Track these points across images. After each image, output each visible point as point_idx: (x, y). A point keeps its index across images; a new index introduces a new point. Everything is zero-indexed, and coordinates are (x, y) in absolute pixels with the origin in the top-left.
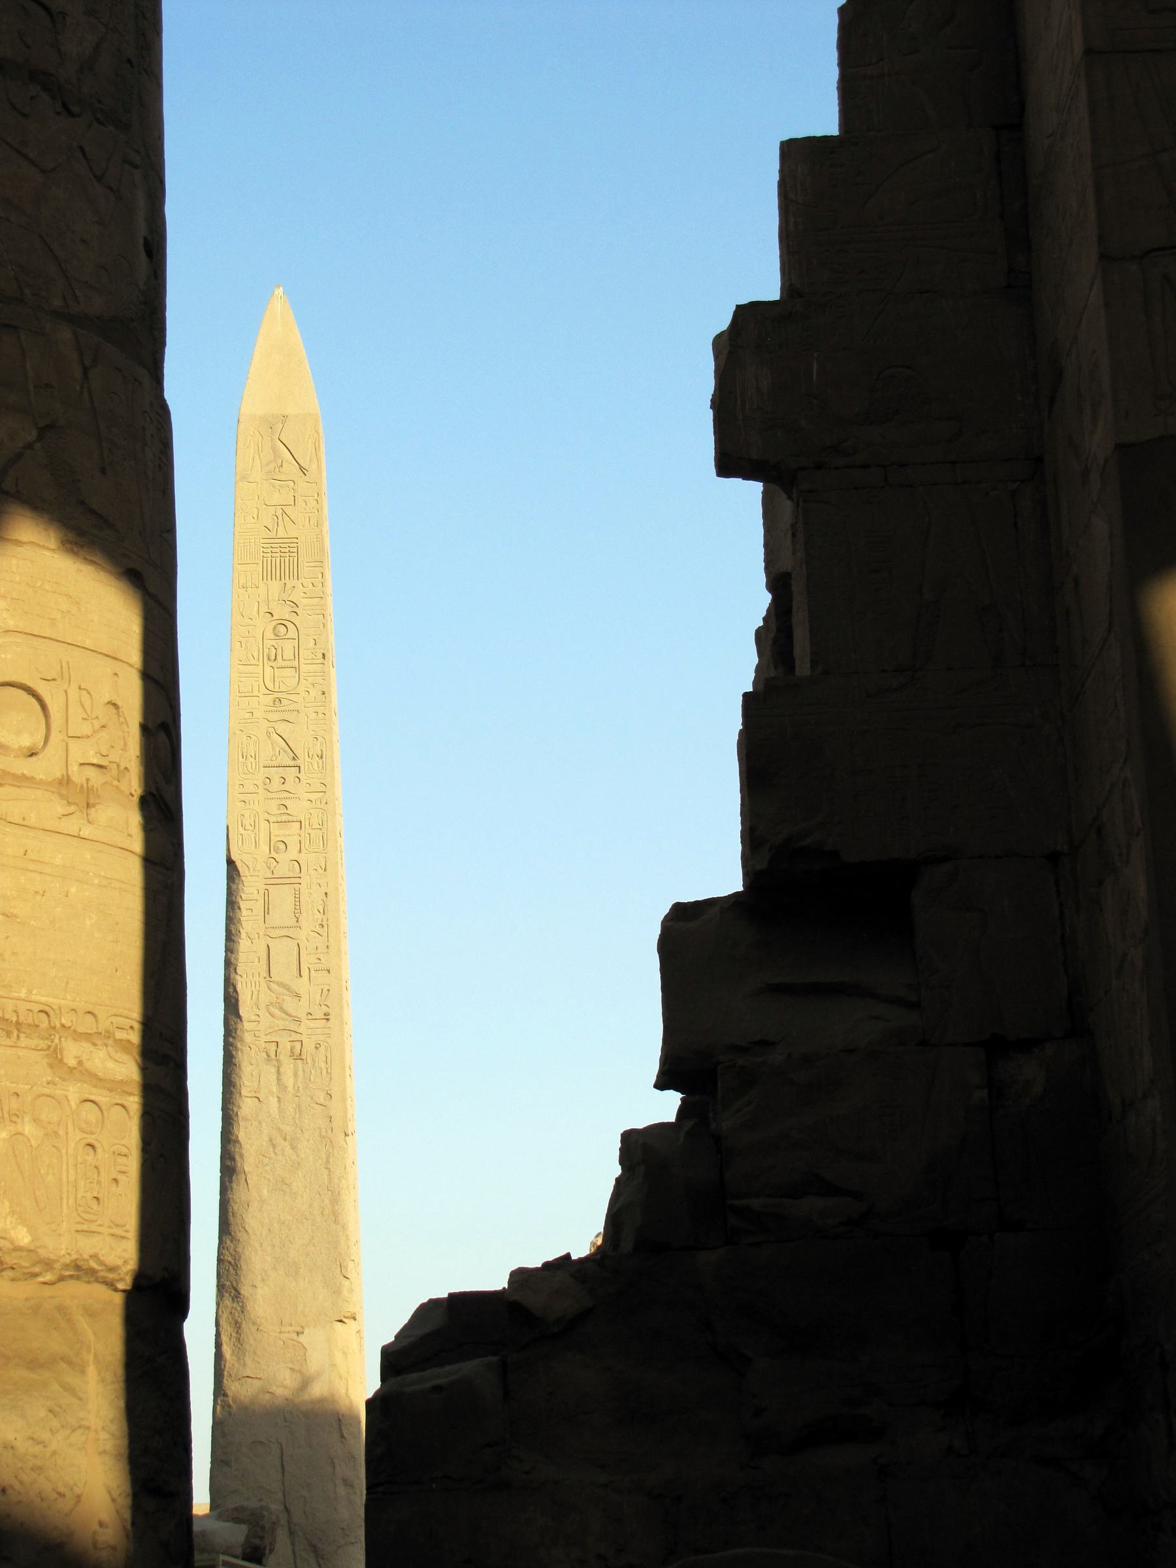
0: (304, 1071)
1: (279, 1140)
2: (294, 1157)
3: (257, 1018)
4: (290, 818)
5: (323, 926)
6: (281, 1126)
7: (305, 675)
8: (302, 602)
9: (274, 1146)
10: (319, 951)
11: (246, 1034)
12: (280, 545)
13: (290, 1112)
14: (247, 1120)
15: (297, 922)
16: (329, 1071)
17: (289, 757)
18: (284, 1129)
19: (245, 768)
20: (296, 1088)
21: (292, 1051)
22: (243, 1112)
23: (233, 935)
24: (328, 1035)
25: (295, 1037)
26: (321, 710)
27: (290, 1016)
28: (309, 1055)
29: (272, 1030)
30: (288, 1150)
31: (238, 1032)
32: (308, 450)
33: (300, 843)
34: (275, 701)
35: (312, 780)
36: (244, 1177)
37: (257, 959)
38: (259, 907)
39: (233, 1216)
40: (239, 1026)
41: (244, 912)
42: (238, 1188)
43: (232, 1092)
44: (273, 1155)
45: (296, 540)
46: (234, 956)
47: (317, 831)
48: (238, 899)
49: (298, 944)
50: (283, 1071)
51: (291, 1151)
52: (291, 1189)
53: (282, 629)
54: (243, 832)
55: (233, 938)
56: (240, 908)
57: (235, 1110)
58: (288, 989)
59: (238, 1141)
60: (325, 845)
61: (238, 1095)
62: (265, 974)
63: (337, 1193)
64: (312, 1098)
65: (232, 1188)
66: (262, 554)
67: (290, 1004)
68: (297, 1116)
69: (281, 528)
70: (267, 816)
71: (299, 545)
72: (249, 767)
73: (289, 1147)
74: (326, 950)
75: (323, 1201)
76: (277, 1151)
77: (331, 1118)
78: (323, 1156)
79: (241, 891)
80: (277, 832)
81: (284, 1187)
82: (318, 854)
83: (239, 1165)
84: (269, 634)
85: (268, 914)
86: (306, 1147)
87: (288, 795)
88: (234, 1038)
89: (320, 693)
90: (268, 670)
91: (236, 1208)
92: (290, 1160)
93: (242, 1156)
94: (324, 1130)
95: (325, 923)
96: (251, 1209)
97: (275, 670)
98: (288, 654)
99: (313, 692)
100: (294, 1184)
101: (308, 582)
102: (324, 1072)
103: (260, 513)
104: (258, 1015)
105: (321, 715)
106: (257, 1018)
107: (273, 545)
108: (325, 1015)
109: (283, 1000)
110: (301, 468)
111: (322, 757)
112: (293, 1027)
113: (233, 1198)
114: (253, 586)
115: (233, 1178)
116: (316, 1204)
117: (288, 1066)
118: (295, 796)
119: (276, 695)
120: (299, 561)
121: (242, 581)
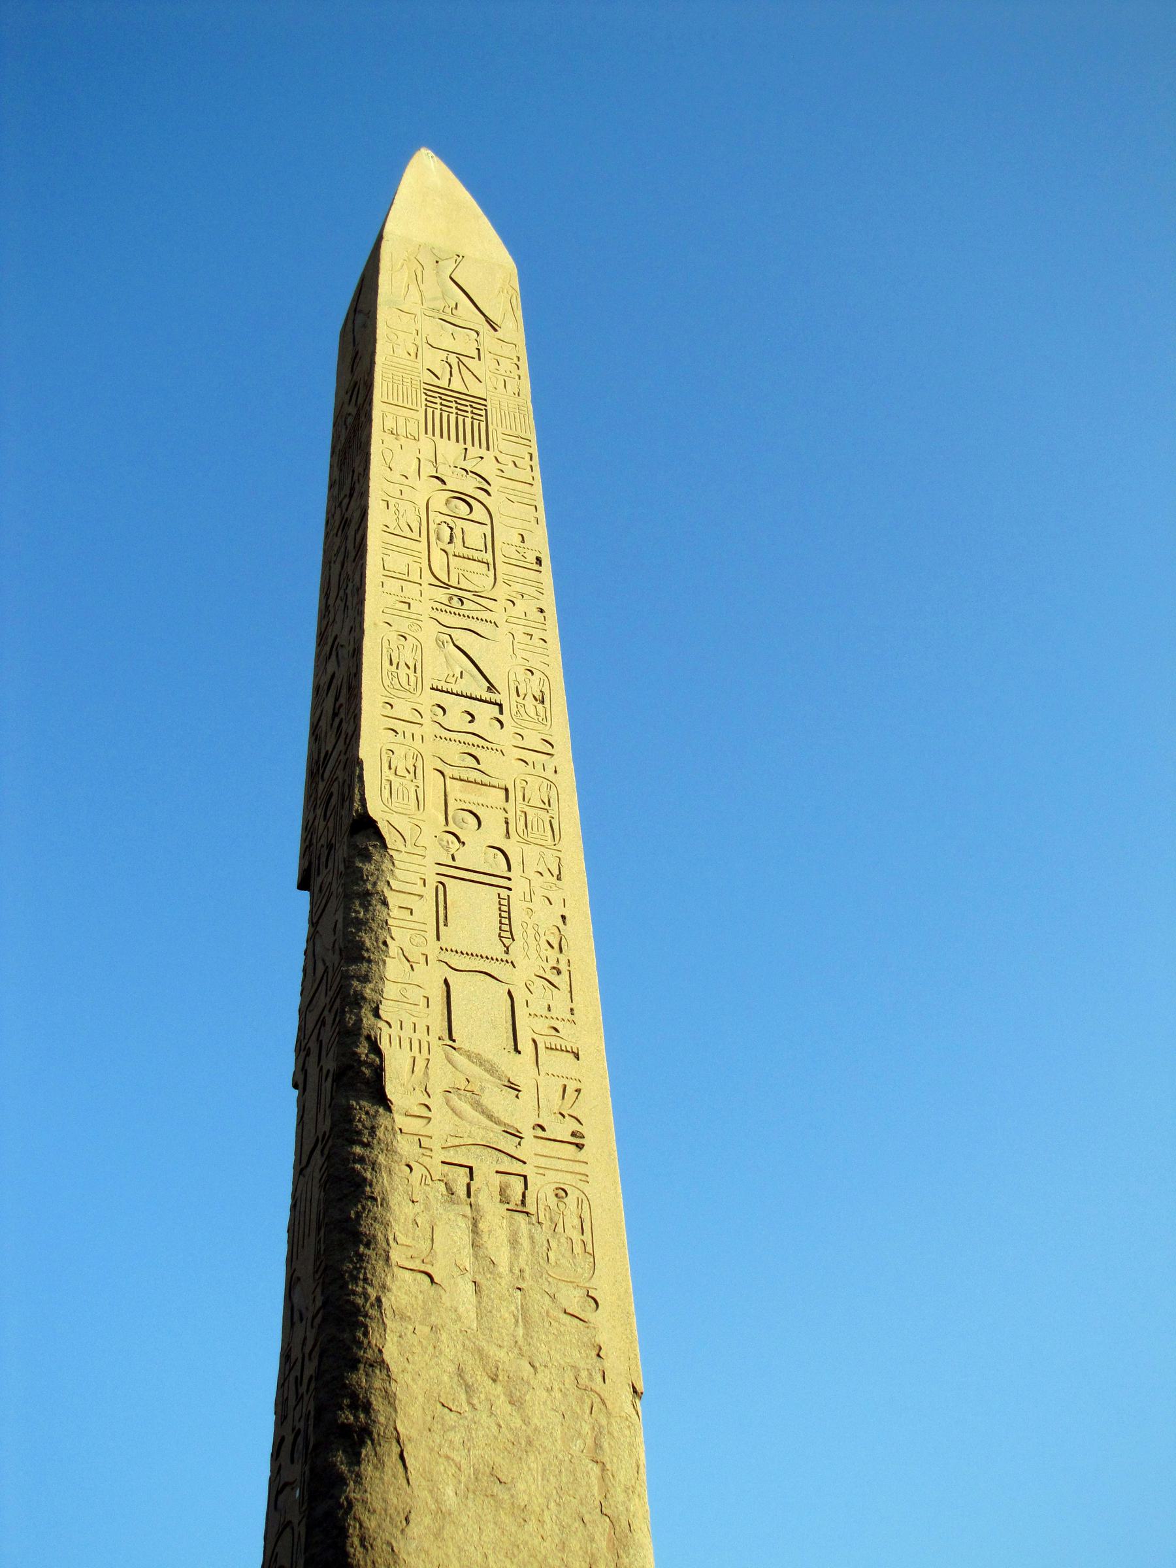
0: (532, 1238)
1: (481, 1379)
2: (517, 1422)
3: (425, 1112)
4: (486, 780)
5: (559, 972)
6: (484, 1344)
9: (469, 1389)
10: (554, 1013)
11: (399, 1136)
13: (505, 1320)
14: (403, 1317)
15: (507, 952)
16: (589, 1249)
18: (491, 1353)
20: (517, 1272)
21: (502, 1191)
22: (393, 1298)
23: (367, 950)
24: (584, 1178)
25: (507, 1165)
26: (537, 634)
27: (498, 1122)
28: (541, 1207)
29: (457, 1141)
30: (502, 1402)
31: (380, 1133)
33: (507, 823)
36: (396, 1450)
37: (423, 1002)
38: (425, 910)
39: (363, 1545)
40: (383, 1120)
41: (395, 912)
42: (377, 1474)
43: (361, 1257)
44: (466, 1407)
46: (371, 985)
47: (540, 812)
48: (381, 886)
49: (509, 993)
50: (486, 1230)
51: (509, 1407)
52: (512, 1496)
54: (392, 777)
55: (366, 955)
56: (385, 903)
57: (372, 1293)
58: (492, 1070)
59: (383, 1361)
60: (557, 838)
61: (381, 1262)
62: (439, 1027)
63: (624, 1524)
64: (553, 1298)
65: (358, 1475)
66: (424, 402)
67: (497, 1100)
68: (521, 1331)
70: (441, 766)
71: (489, 408)
73: (502, 1397)
74: (569, 1016)
75: (592, 1540)
76: (475, 1401)
77: (600, 1348)
78: (586, 1429)
79: (388, 874)
80: (459, 796)
81: (497, 1488)
82: (543, 849)
83: (382, 1419)
85: (446, 925)
86: (545, 1403)
87: (482, 742)
88: (367, 1145)
91: (371, 1524)
92: (508, 1425)
93: (390, 1398)
94: (584, 1374)
95: (563, 966)
96: (414, 1530)
100: (521, 1486)
102: (578, 1249)
103: (420, 350)
104: (427, 1106)
105: (536, 640)
106: (425, 1112)
108: (573, 1134)
109: (482, 1089)
111: (543, 702)
112: (508, 1144)
113: (365, 1502)
115: (364, 1452)
116: (574, 1544)
117: (494, 1217)
118: (494, 747)
119: (452, 591)
120: (490, 429)
121: (390, 424)
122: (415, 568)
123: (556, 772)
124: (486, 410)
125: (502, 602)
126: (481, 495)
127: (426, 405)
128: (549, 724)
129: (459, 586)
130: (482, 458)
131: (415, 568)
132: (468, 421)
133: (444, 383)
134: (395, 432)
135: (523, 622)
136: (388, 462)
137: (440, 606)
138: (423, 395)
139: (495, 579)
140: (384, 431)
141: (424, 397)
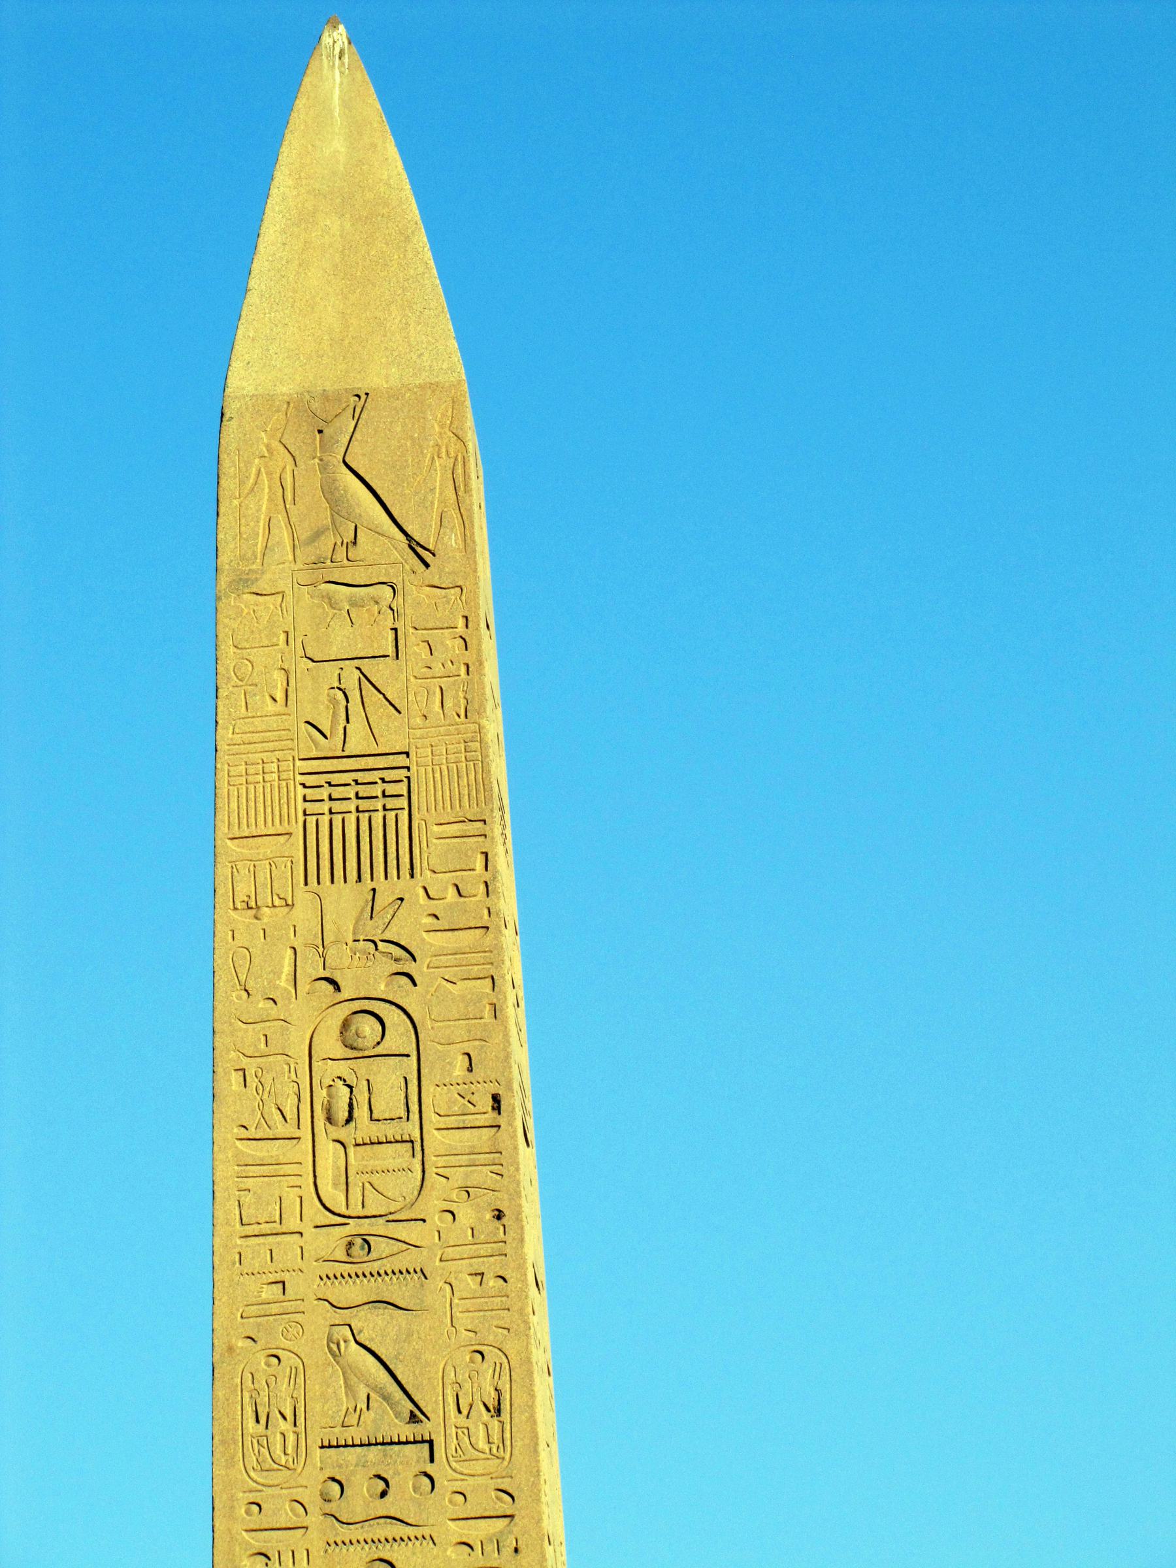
7: (441, 1162)
8: (428, 943)
12: (360, 776)
17: (398, 1415)
19: (264, 1451)
26: (491, 1267)
32: (432, 490)
34: (350, 1244)
35: (471, 1480)
45: (401, 760)
53: (369, 1027)
66: (301, 805)
69: (357, 727)
72: (278, 1451)
84: (329, 1044)
89: (488, 1216)
90: (329, 1153)
97: (351, 1150)
98: (389, 1100)
99: (466, 1215)
101: (441, 885)
105: (492, 1283)
107: (336, 779)
110: (414, 545)
111: (498, 1411)
114: (277, 902)
118: (418, 1532)
119: (353, 1227)
121: (244, 889)
122: (291, 1197)
123: (516, 1550)
124: (408, 778)
125: (437, 1220)
126: (403, 992)
127: (305, 814)
128: (507, 1456)
129: (362, 1214)
130: (402, 899)
131: (291, 1197)
132: (378, 818)
133: (334, 745)
134: (253, 904)
135: (467, 1251)
136: (243, 977)
137: (331, 1268)
138: (300, 788)
139: (423, 1171)
140: (235, 909)
141: (301, 791)
